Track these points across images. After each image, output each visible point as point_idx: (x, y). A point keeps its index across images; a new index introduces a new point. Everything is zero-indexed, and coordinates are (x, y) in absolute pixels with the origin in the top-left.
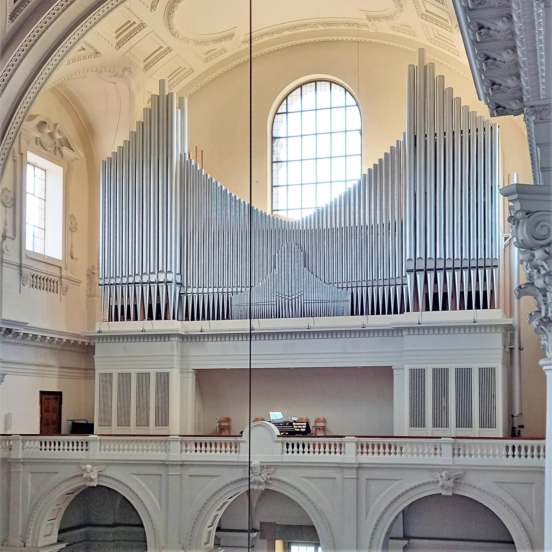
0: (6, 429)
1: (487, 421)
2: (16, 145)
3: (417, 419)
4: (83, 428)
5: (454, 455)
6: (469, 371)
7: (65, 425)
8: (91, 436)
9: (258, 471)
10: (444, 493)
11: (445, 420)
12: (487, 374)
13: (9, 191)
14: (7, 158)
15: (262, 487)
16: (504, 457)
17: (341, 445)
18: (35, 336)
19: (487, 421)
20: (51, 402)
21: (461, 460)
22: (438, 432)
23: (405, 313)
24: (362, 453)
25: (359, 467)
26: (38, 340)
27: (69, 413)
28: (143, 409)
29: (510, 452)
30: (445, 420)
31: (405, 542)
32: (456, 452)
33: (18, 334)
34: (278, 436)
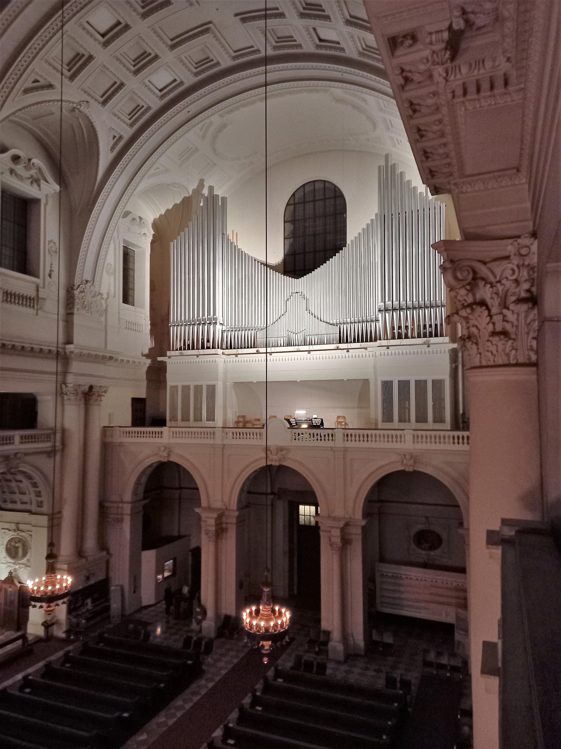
0: (110, 422)
1: (438, 419)
2: (115, 234)
3: (388, 417)
4: (160, 422)
5: (414, 442)
6: (425, 382)
7: (147, 420)
8: (164, 428)
9: (274, 452)
10: (407, 469)
11: (407, 418)
12: (438, 385)
13: (111, 265)
14: (109, 243)
15: (277, 464)
16: (452, 444)
17: (332, 435)
18: (128, 361)
19: (438, 419)
20: (138, 405)
21: (419, 446)
22: (402, 425)
23: (378, 341)
24: (348, 440)
25: (346, 450)
26: (118, 362)
27: (150, 411)
28: (198, 409)
29: (456, 441)
30: (407, 418)
31: (380, 504)
32: (416, 440)
33: (117, 360)
34: (288, 428)
